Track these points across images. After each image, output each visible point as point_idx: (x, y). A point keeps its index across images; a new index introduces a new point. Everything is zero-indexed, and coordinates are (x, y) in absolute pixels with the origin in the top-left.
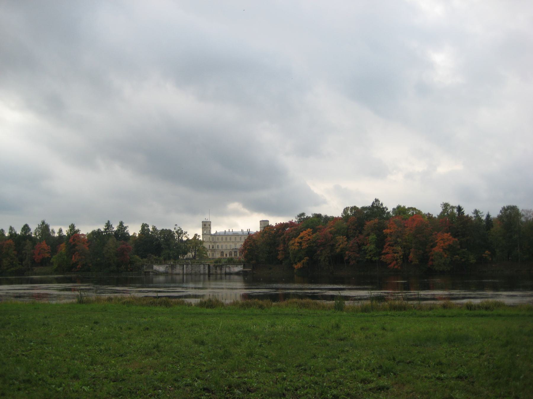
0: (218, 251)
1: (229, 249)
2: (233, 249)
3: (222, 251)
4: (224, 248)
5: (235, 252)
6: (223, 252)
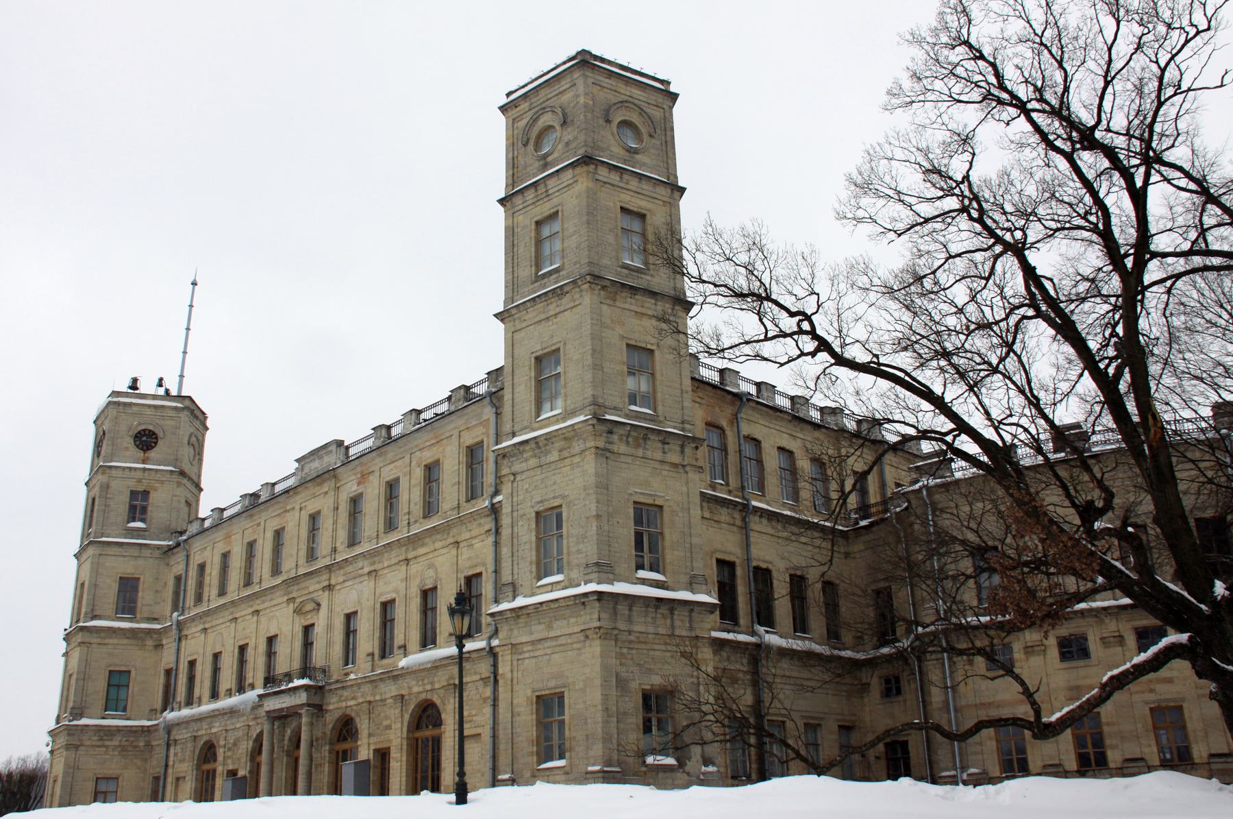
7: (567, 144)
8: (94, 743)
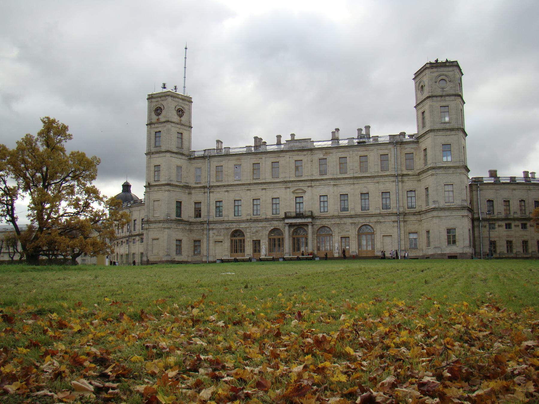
0: (218, 226)
1: (269, 215)
3: (235, 227)
4: (246, 211)
5: (295, 232)
6: (237, 233)
7: (451, 87)
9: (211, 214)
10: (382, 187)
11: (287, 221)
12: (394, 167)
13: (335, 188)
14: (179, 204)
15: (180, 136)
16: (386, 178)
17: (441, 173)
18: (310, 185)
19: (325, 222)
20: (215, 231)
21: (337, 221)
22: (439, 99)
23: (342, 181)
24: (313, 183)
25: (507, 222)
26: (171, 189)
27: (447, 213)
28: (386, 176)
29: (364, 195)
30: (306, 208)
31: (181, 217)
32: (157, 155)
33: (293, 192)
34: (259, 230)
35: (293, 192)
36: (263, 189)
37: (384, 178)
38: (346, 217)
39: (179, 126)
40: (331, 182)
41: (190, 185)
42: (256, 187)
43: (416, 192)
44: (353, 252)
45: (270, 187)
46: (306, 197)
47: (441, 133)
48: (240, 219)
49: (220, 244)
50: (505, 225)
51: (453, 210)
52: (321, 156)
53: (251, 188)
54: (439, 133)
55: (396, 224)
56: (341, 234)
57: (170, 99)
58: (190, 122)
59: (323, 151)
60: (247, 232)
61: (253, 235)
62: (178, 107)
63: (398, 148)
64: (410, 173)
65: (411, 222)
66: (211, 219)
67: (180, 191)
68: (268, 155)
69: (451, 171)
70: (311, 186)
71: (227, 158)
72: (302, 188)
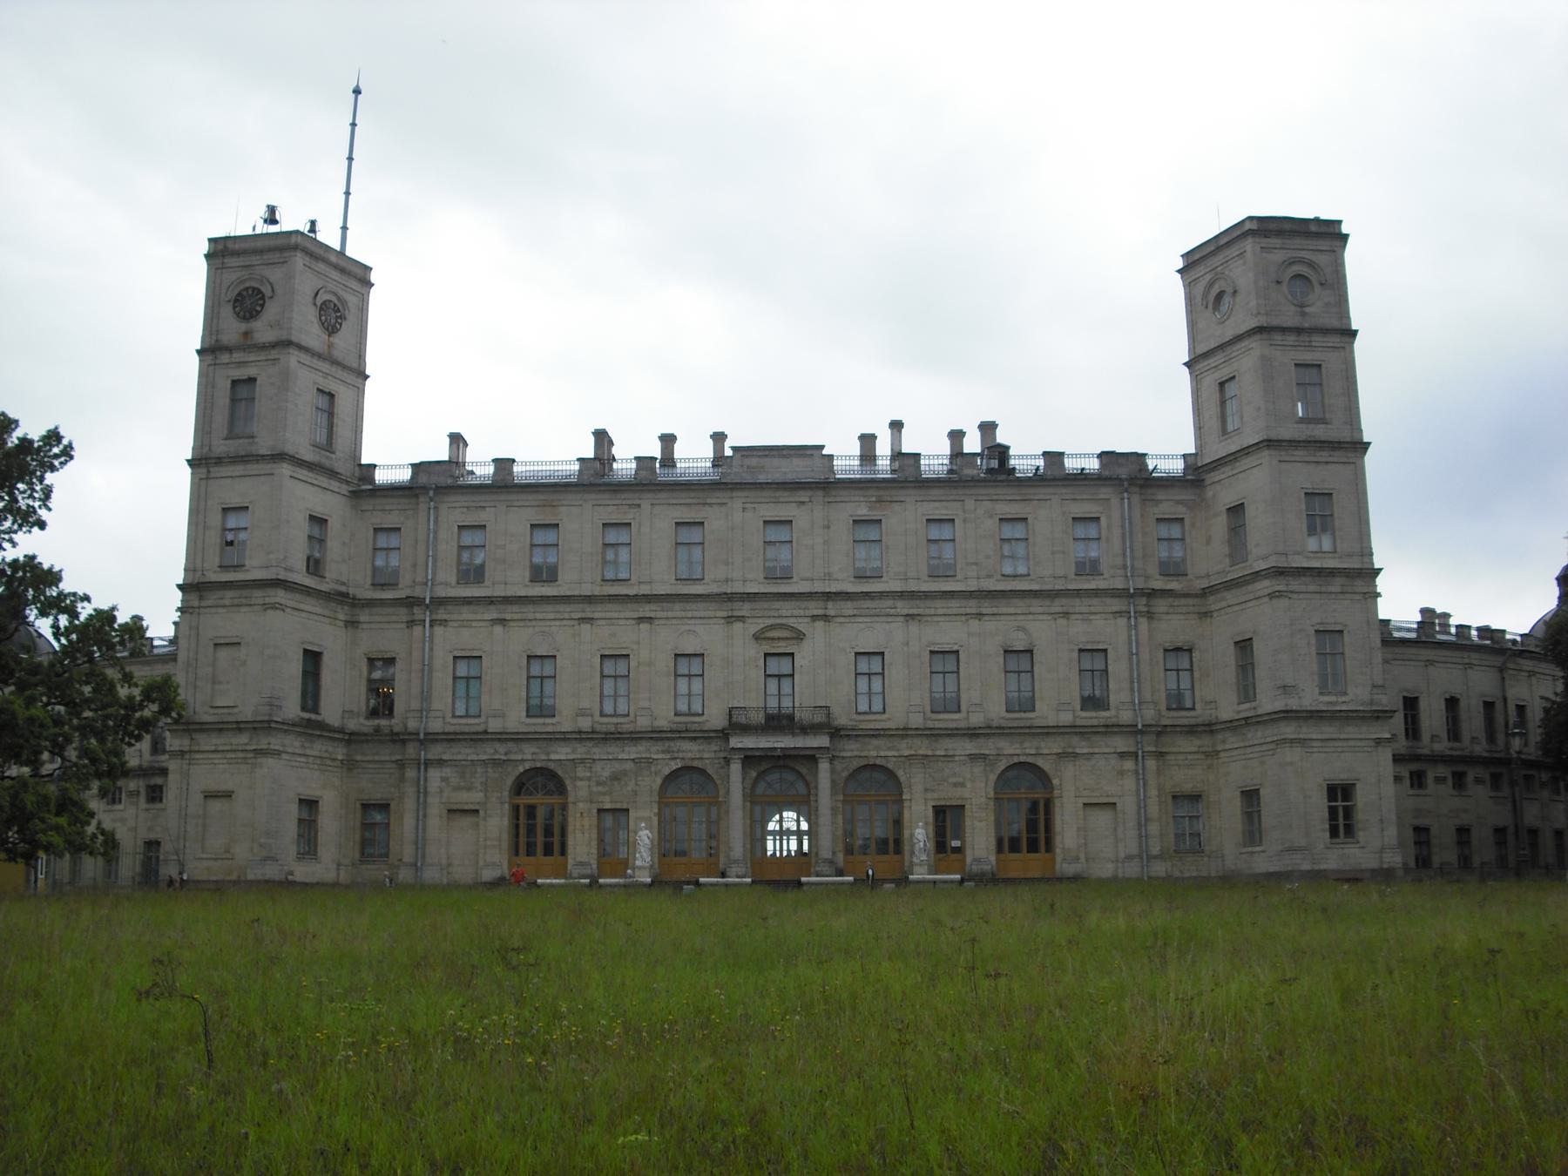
0: (466, 753)
2: (735, 725)
3: (529, 755)
6: (546, 780)
7: (1327, 304)
8: (297, 751)
9: (436, 705)
10: (1081, 631)
11: (735, 742)
12: (1119, 561)
13: (914, 627)
14: (313, 659)
15: (323, 402)
16: (1095, 601)
17: (1303, 588)
18: (820, 612)
19: (877, 748)
20: (447, 771)
21: (923, 749)
22: (1291, 339)
23: (939, 603)
24: (830, 604)
25: (1415, 767)
26: (290, 603)
27: (1328, 730)
28: (1096, 593)
29: (1020, 657)
30: (803, 697)
31: (317, 713)
32: (239, 469)
33: (757, 637)
34: (625, 773)
35: (757, 637)
36: (641, 620)
37: (1087, 601)
38: (954, 733)
39: (325, 367)
40: (900, 604)
41: (351, 591)
42: (613, 611)
43: (1196, 655)
44: (977, 860)
45: (670, 614)
46: (805, 655)
47: (1299, 454)
48: (550, 729)
49: (467, 821)
50: (1407, 775)
51: (1347, 718)
52: (863, 511)
53: (596, 615)
54: (1296, 453)
55: (1129, 765)
56: (936, 795)
57: (299, 260)
58: (361, 357)
59: (871, 492)
60: (575, 778)
61: (600, 789)
62: (323, 297)
63: (1136, 499)
64: (1174, 585)
65: (1181, 757)
66: (436, 726)
67: (318, 610)
68: (664, 495)
69: (1336, 585)
70: (826, 618)
71: (503, 497)
72: (791, 622)
